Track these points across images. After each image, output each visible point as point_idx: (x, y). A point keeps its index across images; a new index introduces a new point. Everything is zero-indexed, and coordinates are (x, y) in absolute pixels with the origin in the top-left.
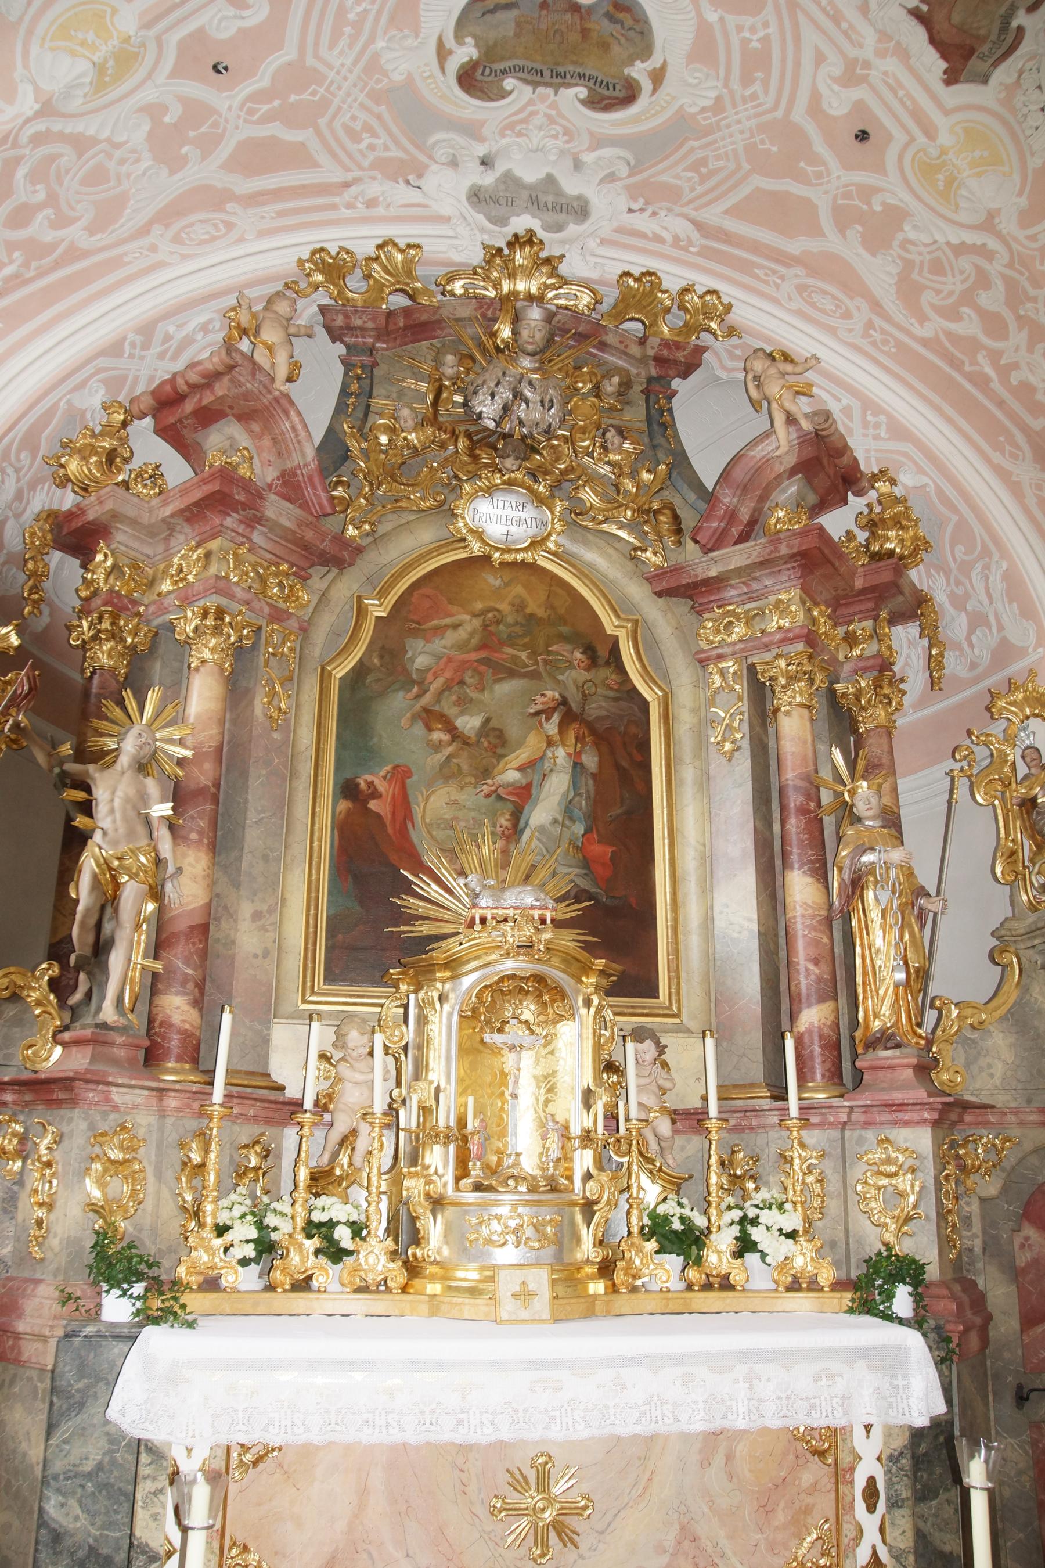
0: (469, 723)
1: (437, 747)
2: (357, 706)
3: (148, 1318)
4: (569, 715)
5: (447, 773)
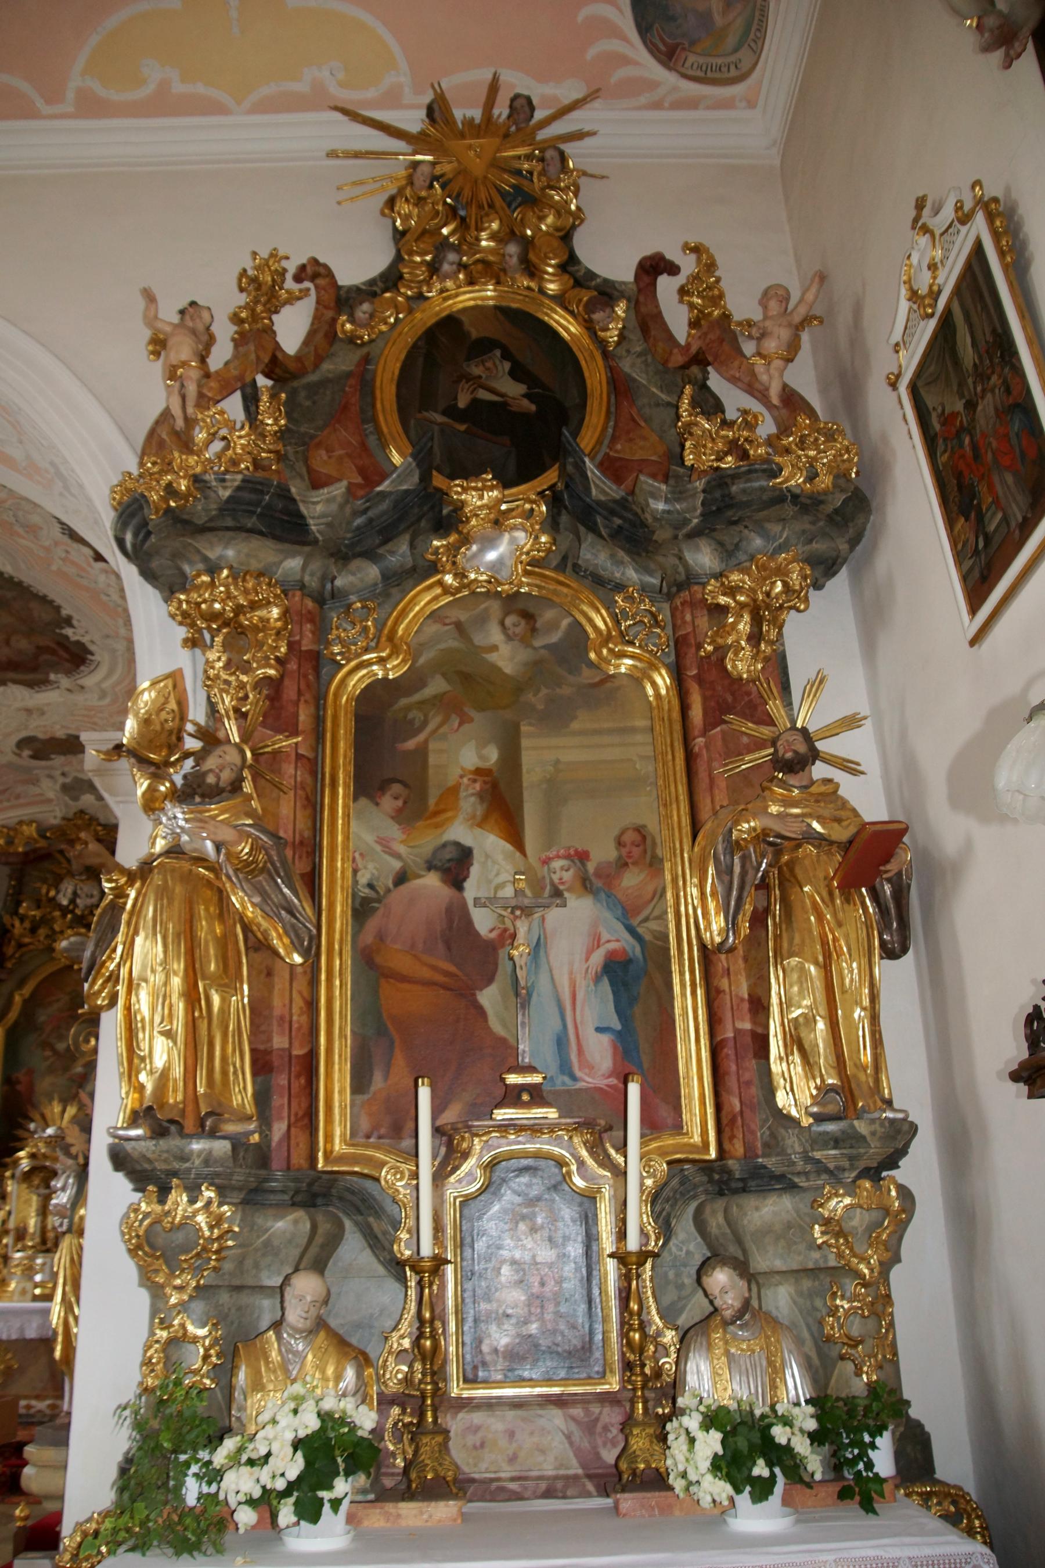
1: (46, 1059)
5: (51, 1070)
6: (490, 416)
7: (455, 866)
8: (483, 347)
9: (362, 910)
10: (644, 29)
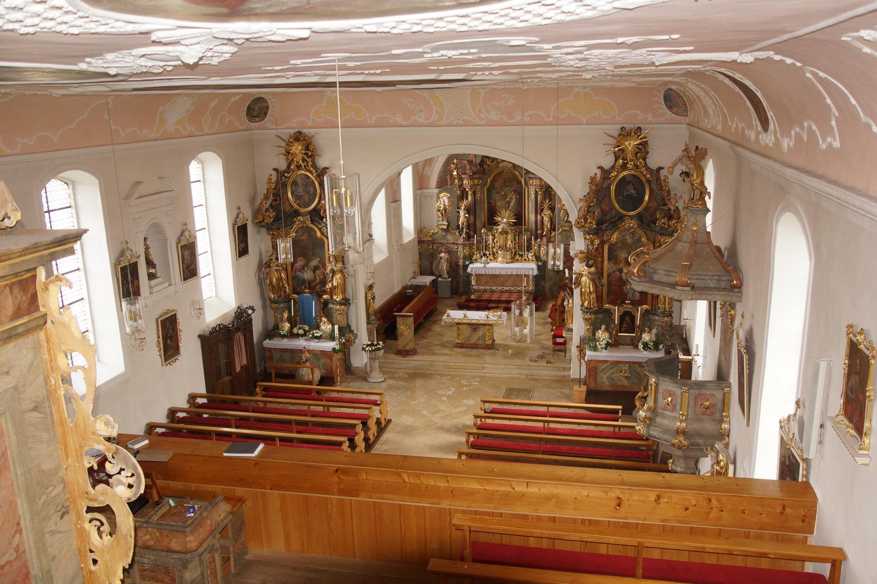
0: (503, 193)
2: (489, 190)
3: (471, 263)
4: (515, 191)
5: (500, 200)
6: (629, 197)
7: (621, 271)
8: (629, 183)
9: (608, 276)
10: (665, 102)
